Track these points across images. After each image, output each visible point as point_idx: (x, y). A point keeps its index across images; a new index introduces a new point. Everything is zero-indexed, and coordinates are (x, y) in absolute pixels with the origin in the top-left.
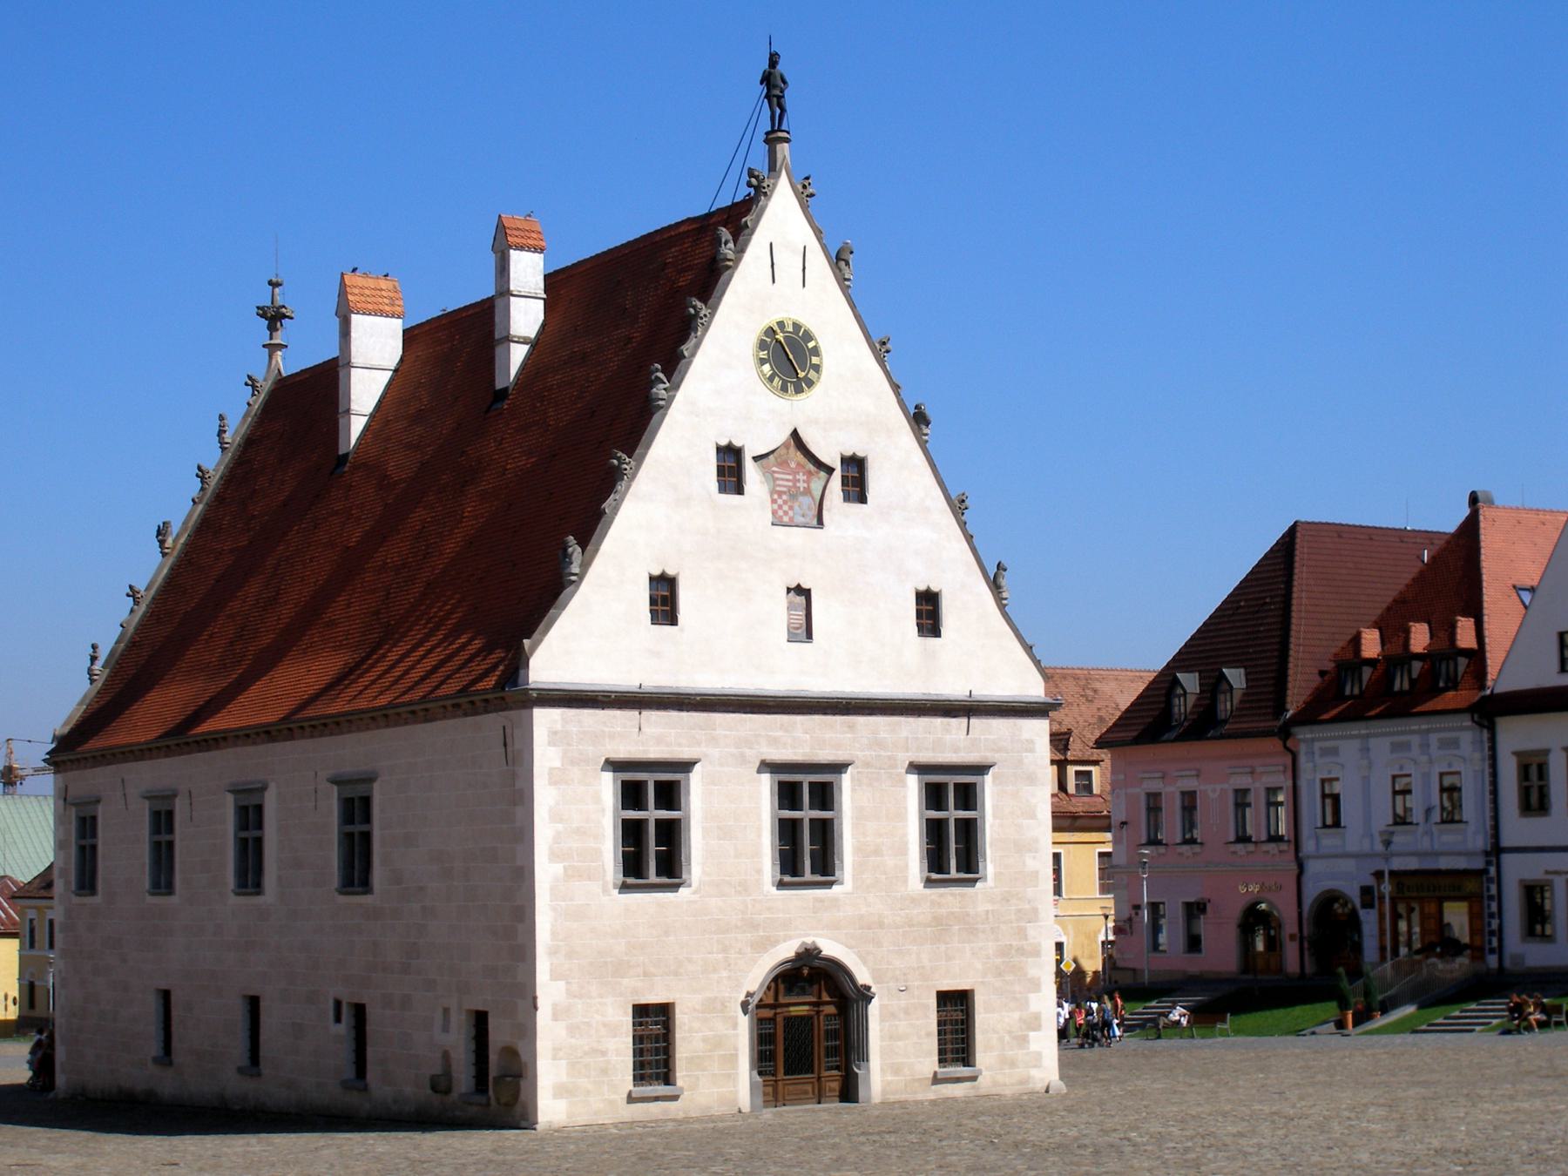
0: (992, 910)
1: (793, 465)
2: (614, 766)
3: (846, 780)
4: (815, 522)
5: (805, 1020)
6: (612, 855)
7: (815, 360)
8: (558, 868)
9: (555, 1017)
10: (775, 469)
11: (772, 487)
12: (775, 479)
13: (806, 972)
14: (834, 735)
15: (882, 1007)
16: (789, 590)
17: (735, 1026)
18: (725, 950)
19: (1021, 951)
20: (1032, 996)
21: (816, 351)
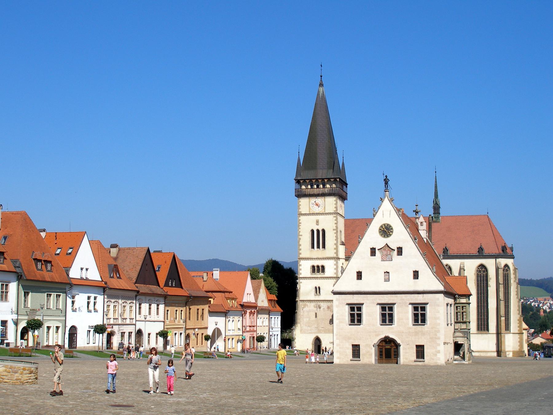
0: (429, 331)
1: (387, 250)
2: (348, 304)
3: (395, 306)
4: (391, 260)
6: (348, 319)
7: (391, 230)
8: (338, 321)
9: (337, 346)
13: (387, 340)
15: (403, 347)
16: (385, 273)
17: (372, 349)
19: (436, 338)
20: (438, 347)
21: (392, 229)
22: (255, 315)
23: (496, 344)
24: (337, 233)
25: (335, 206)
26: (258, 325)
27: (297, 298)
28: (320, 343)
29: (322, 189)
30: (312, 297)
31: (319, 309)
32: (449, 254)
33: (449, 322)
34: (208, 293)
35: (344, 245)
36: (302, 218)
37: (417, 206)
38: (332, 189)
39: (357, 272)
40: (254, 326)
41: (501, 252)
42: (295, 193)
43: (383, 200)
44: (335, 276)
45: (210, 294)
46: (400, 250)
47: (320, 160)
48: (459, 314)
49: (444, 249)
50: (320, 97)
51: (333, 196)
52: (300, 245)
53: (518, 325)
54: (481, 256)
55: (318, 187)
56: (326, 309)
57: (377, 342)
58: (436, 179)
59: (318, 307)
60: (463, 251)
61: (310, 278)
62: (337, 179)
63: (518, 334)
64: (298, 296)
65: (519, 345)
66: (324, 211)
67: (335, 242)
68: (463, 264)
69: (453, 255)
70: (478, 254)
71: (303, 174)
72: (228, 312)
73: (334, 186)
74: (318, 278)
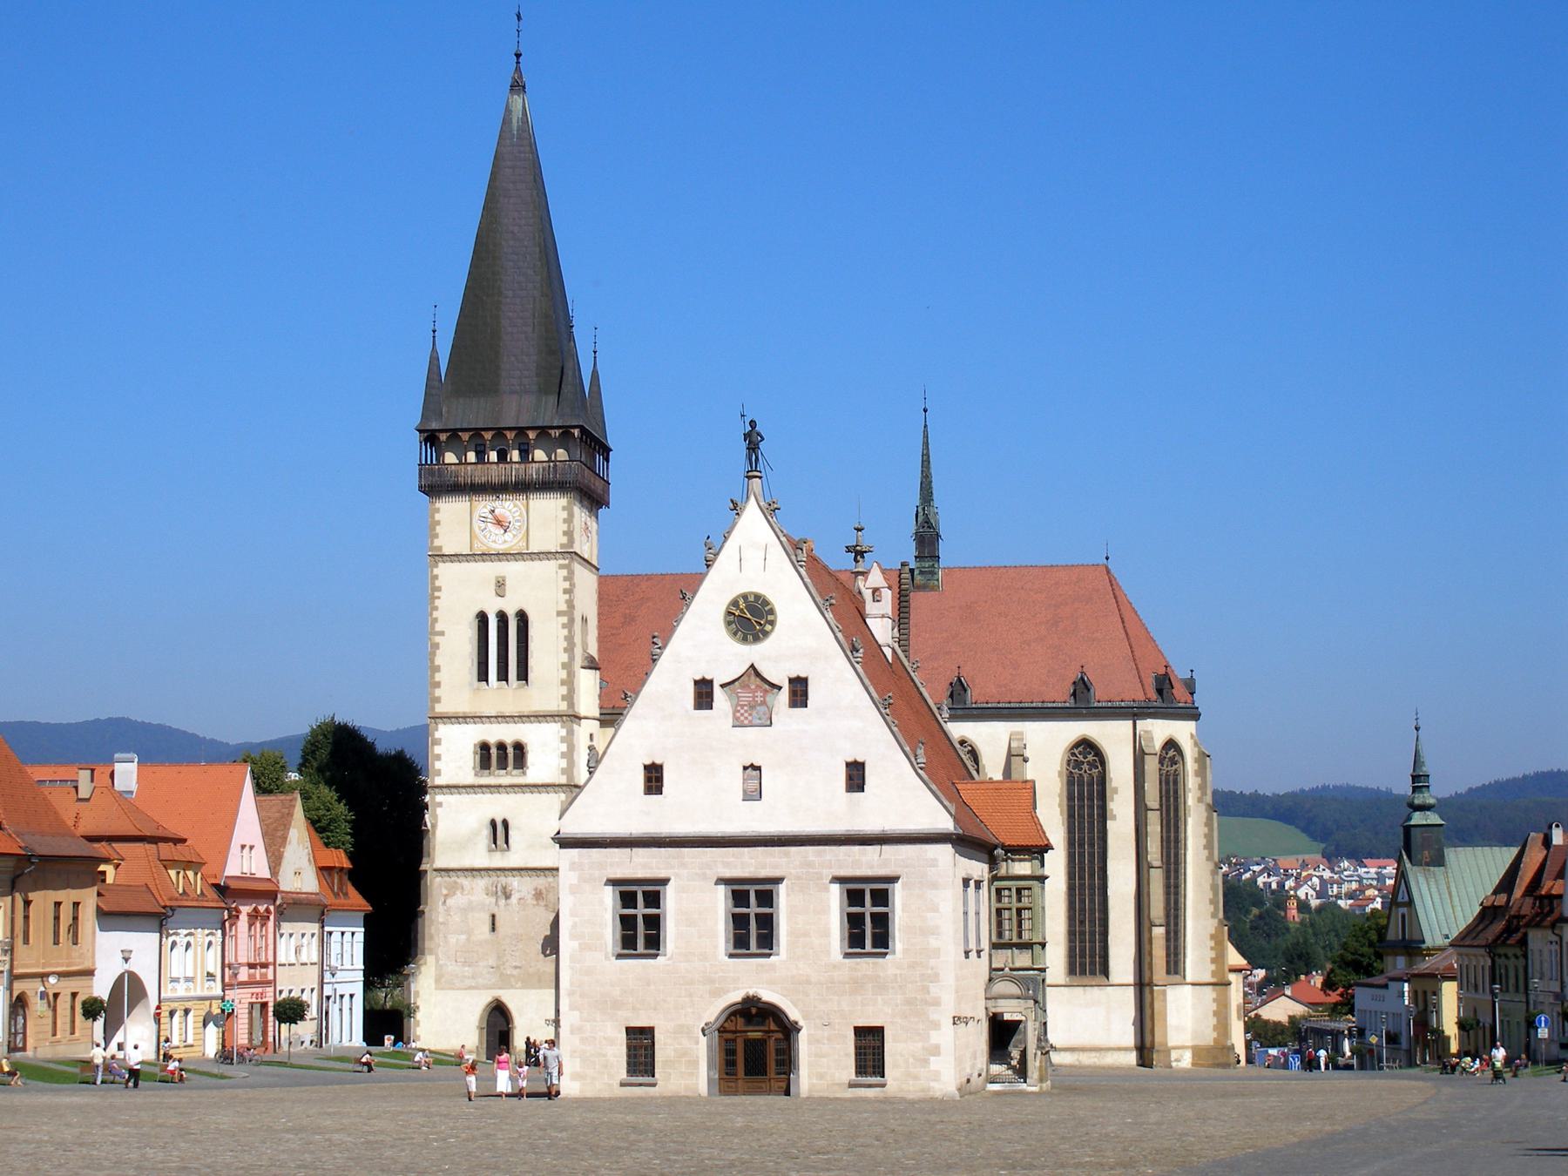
0: (901, 975)
1: (753, 687)
2: (614, 882)
4: (769, 722)
5: (762, 1043)
6: (611, 937)
7: (770, 618)
8: (575, 944)
9: (572, 1032)
10: (739, 691)
11: (735, 702)
12: (738, 697)
13: (754, 1011)
14: (772, 860)
15: (809, 1035)
16: (745, 768)
17: (697, 1043)
18: (691, 995)
19: (926, 1003)
21: (772, 612)
22: (271, 924)
23: (1133, 1024)
24: (569, 625)
25: (565, 527)
26: (281, 959)
27: (425, 860)
28: (508, 1024)
29: (517, 466)
30: (480, 856)
31: (504, 901)
32: (968, 702)
33: (972, 946)
34: (96, 845)
35: (596, 669)
36: (444, 571)
37: (859, 530)
38: (555, 466)
39: (646, 767)
40: (264, 966)
41: (1153, 695)
42: (420, 481)
43: (742, 510)
44: (563, 780)
45: (101, 849)
46: (799, 688)
47: (513, 359)
48: (1006, 914)
49: (951, 684)
50: (511, 131)
51: (556, 491)
52: (437, 669)
53: (1213, 954)
54: (1084, 711)
55: (503, 456)
56: (531, 901)
57: (717, 1019)
58: (926, 436)
59: (499, 893)
60: (1019, 692)
61: (472, 787)
62: (572, 431)
63: (1211, 987)
64: (429, 856)
65: (1214, 1025)
66: (525, 544)
67: (565, 658)
68: (1018, 739)
69: (985, 705)
70: (1071, 703)
71: (448, 412)
72: (170, 913)
73: (561, 454)
74: (501, 789)
